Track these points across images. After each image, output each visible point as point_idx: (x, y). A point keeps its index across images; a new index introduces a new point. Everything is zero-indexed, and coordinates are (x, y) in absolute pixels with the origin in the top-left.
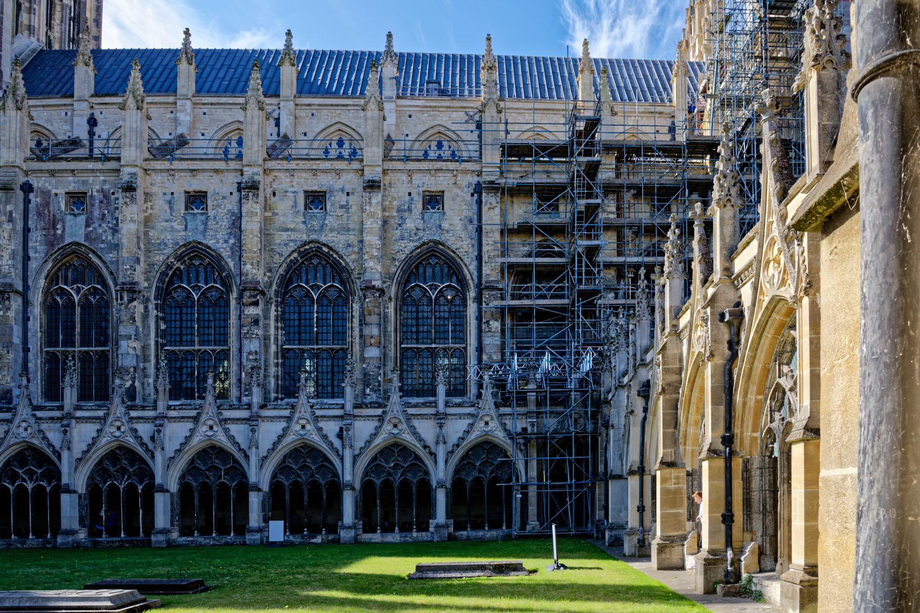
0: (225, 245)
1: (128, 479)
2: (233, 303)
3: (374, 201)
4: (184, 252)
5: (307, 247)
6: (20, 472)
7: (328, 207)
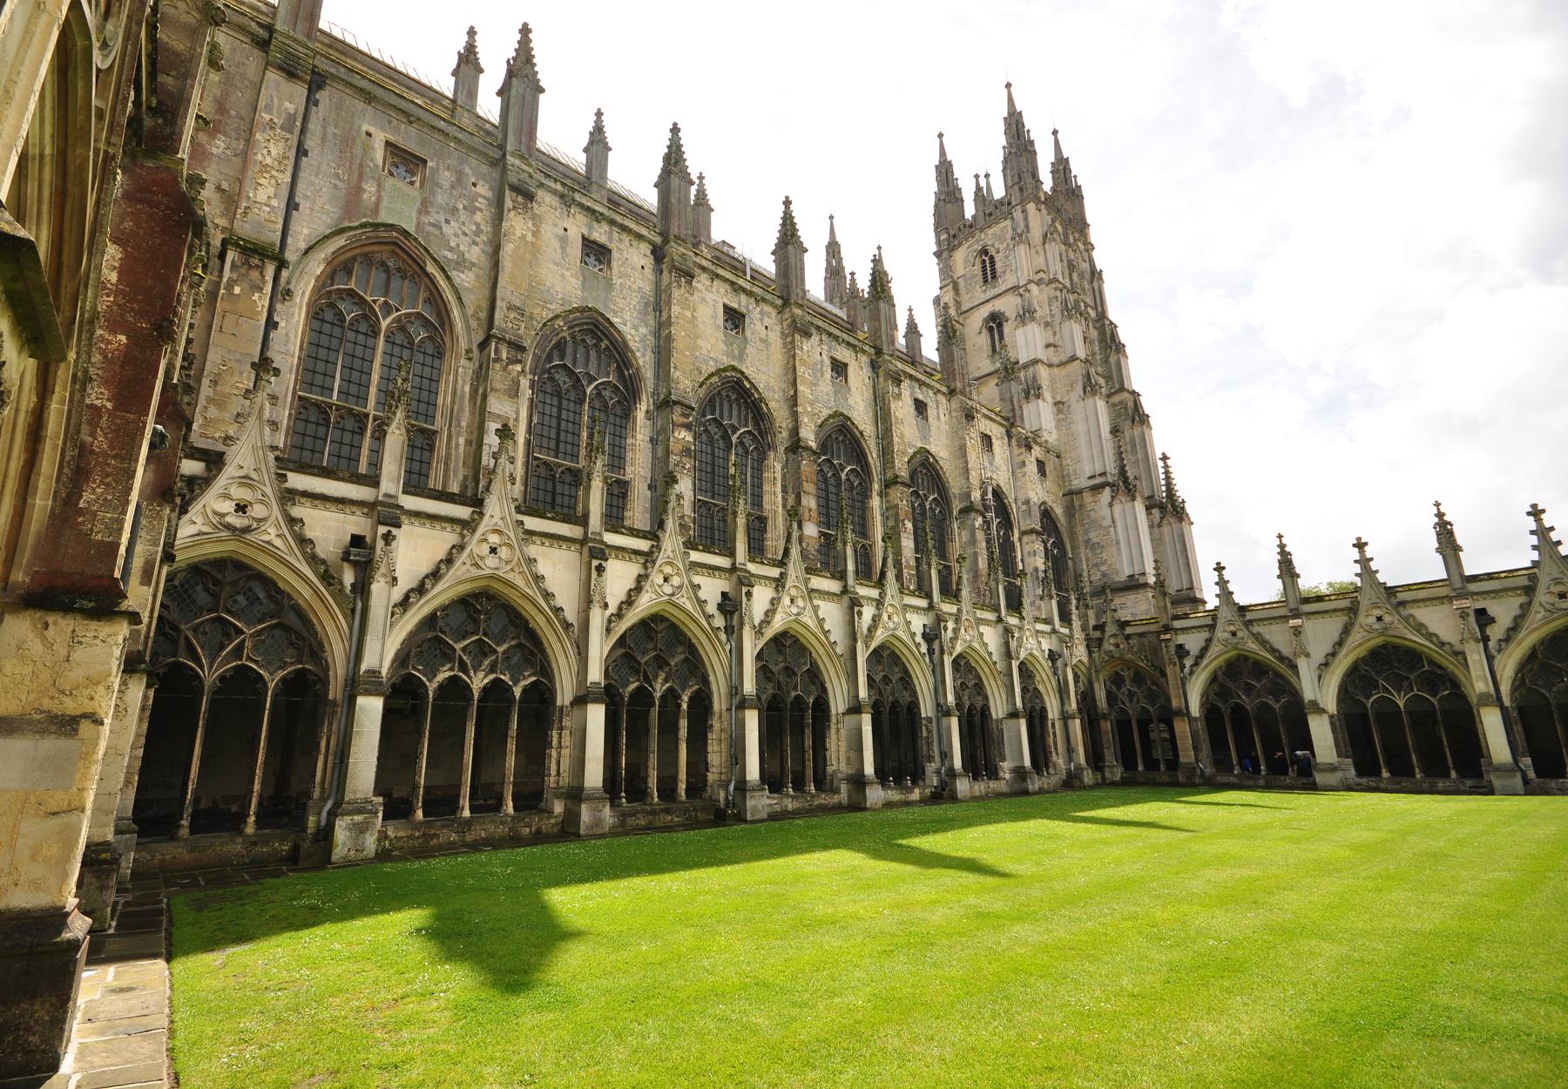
0: (633, 332)
1: (666, 680)
2: (640, 415)
3: (805, 348)
4: (577, 318)
5: (729, 374)
6: (458, 646)
7: (748, 334)
